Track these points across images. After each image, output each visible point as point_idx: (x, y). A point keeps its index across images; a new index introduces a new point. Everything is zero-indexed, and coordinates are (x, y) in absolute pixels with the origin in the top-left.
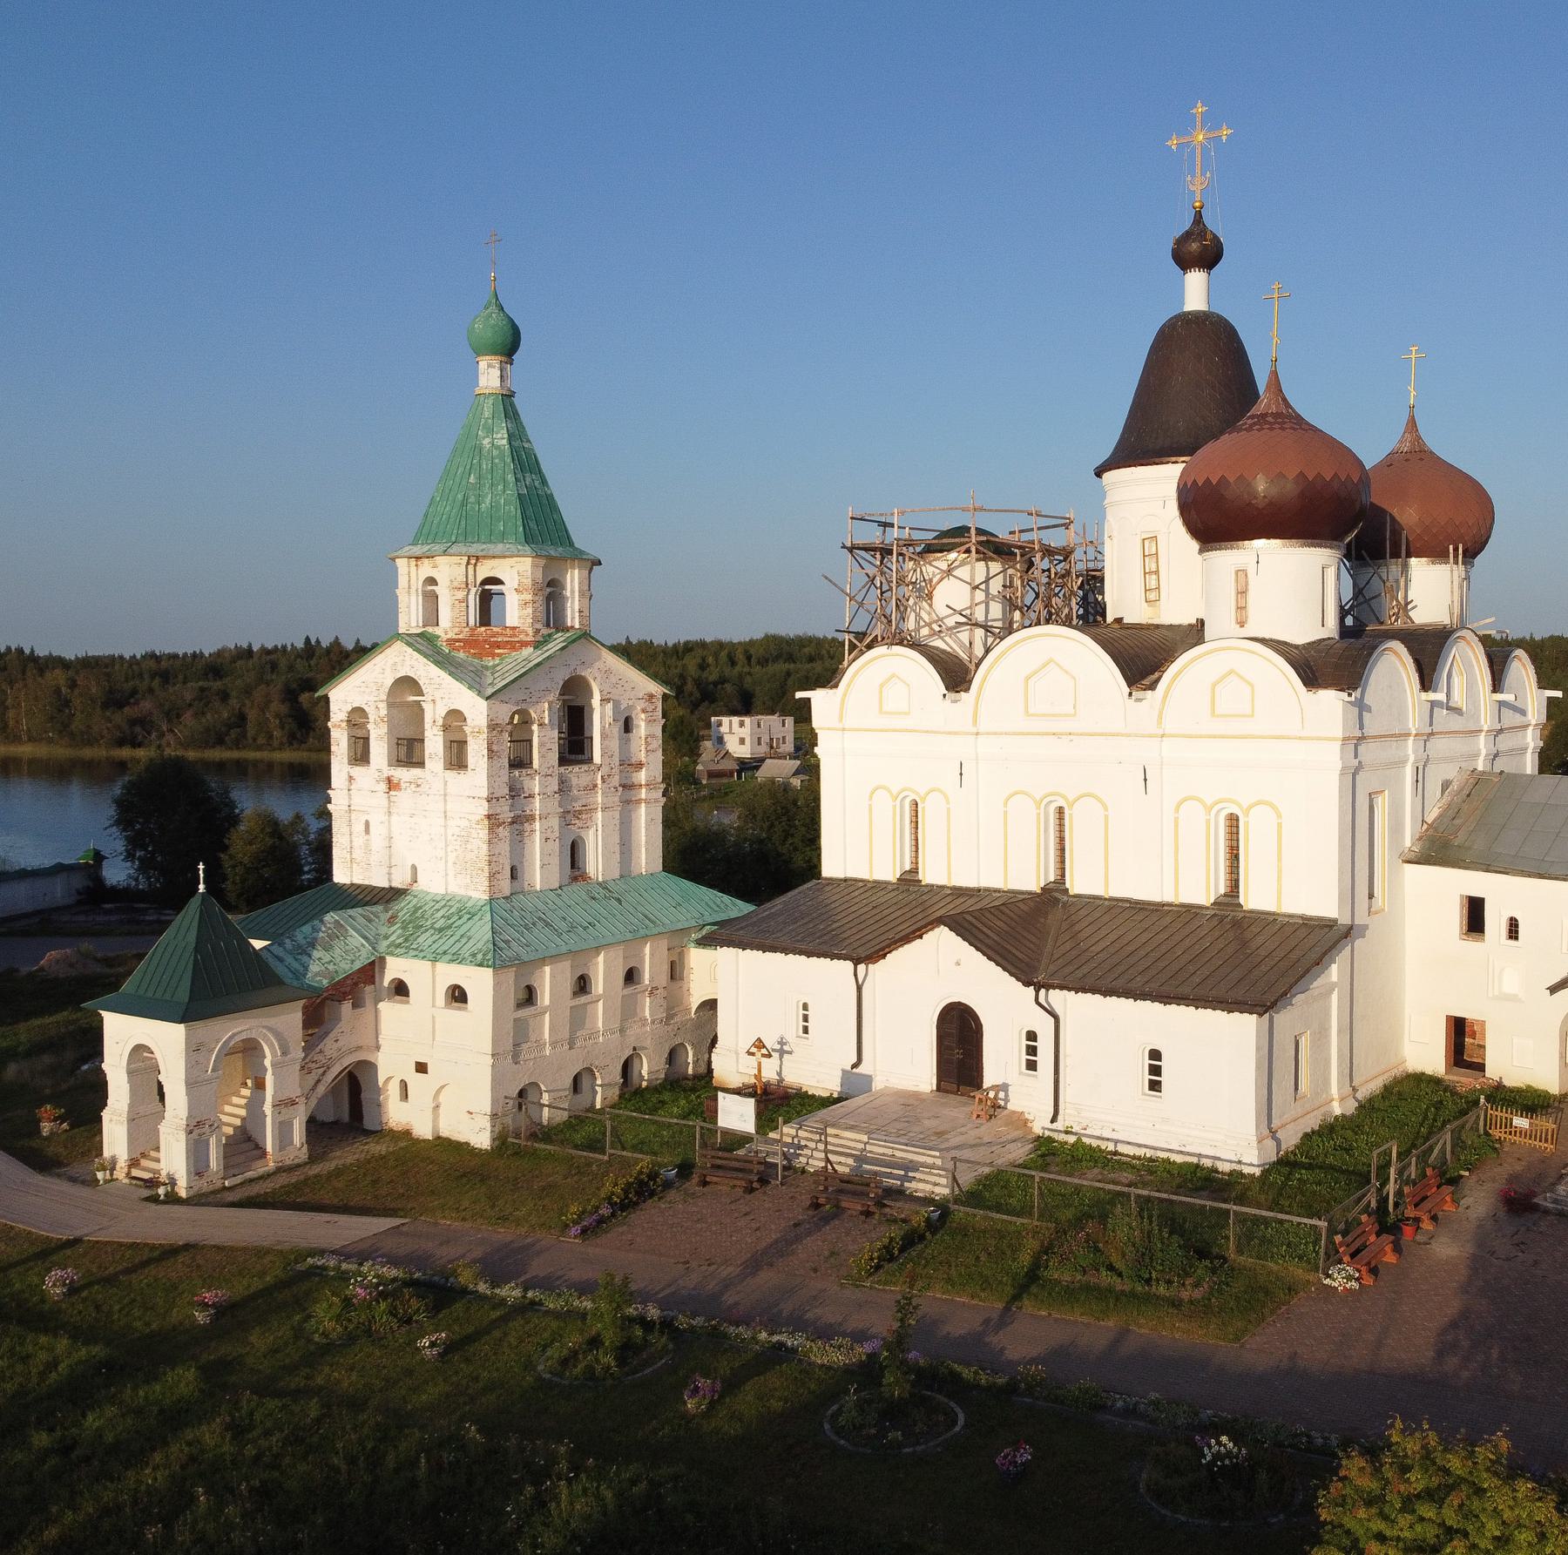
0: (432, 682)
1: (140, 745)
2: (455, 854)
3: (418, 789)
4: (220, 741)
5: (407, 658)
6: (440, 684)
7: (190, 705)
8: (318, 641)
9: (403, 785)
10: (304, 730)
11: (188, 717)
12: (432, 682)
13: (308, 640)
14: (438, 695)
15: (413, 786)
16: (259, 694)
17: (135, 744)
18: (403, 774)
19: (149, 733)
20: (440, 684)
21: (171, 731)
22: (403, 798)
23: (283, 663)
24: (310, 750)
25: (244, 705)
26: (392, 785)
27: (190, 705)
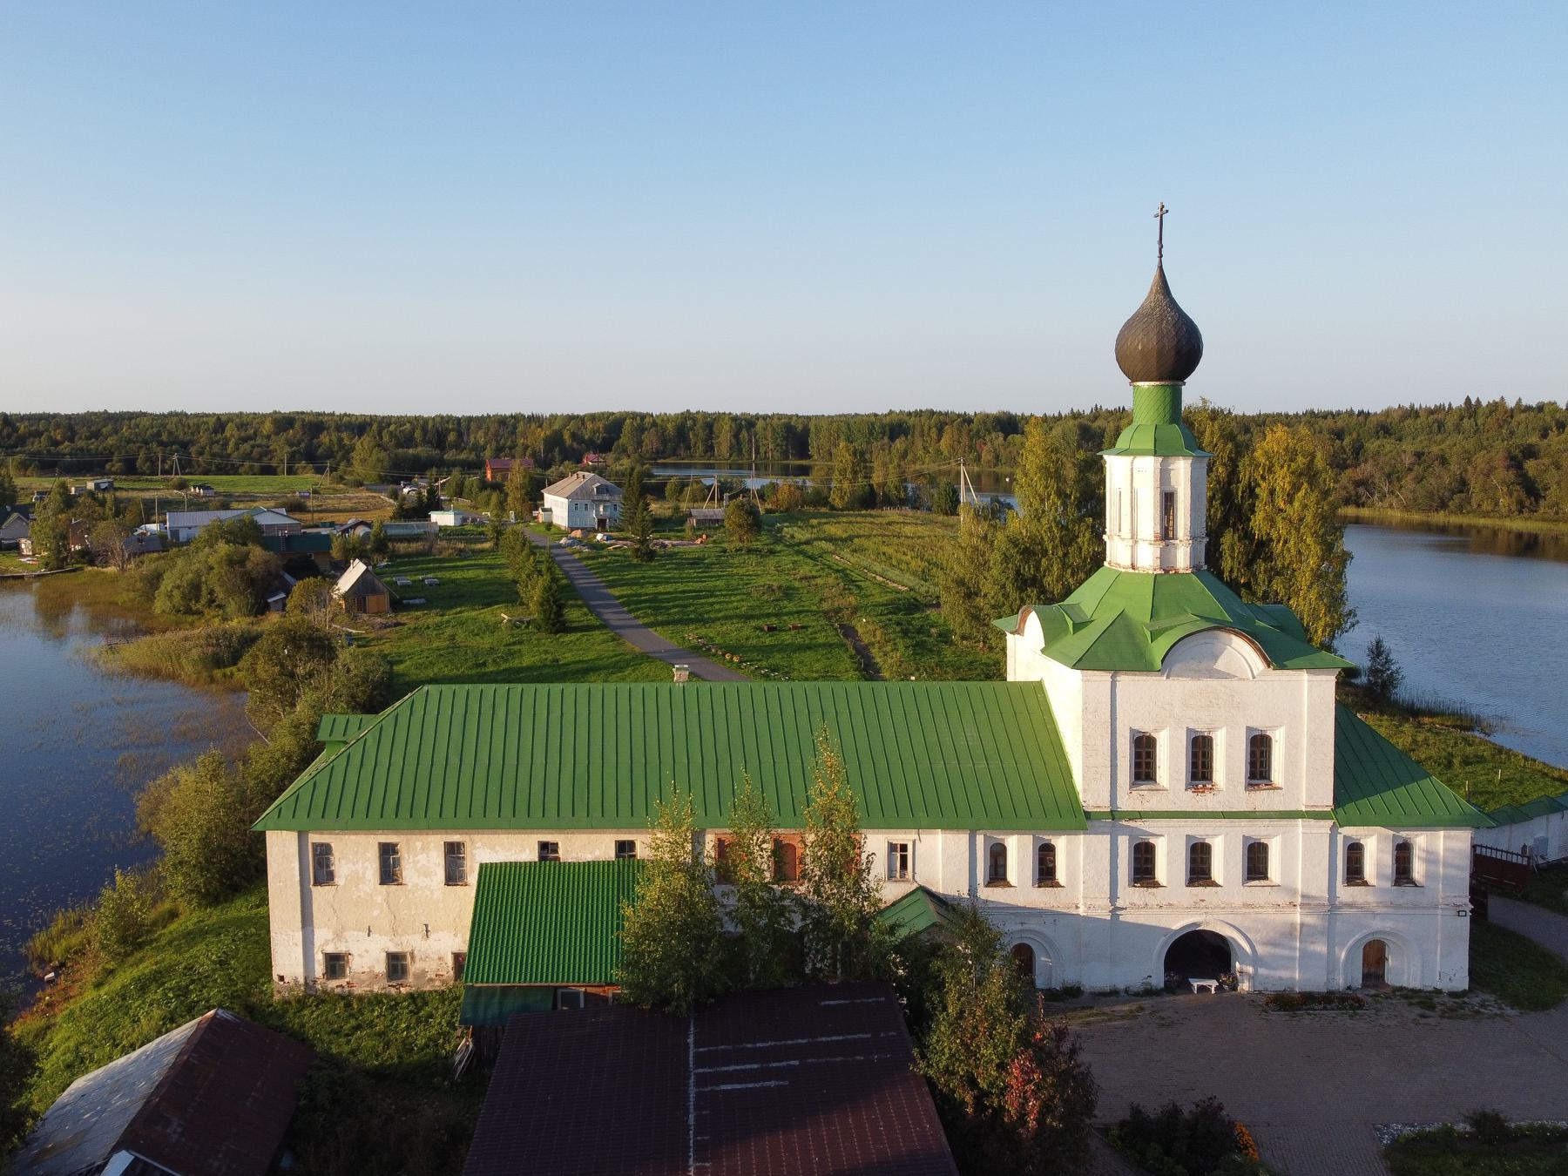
1: (1363, 505)
4: (1443, 505)
7: (1410, 470)
8: (1478, 401)
10: (1533, 499)
11: (1408, 482)
13: (1468, 400)
16: (1480, 459)
17: (1359, 504)
19: (1372, 494)
21: (1393, 493)
23: (1450, 423)
24: (1544, 520)
25: (1466, 470)
27: (1410, 470)
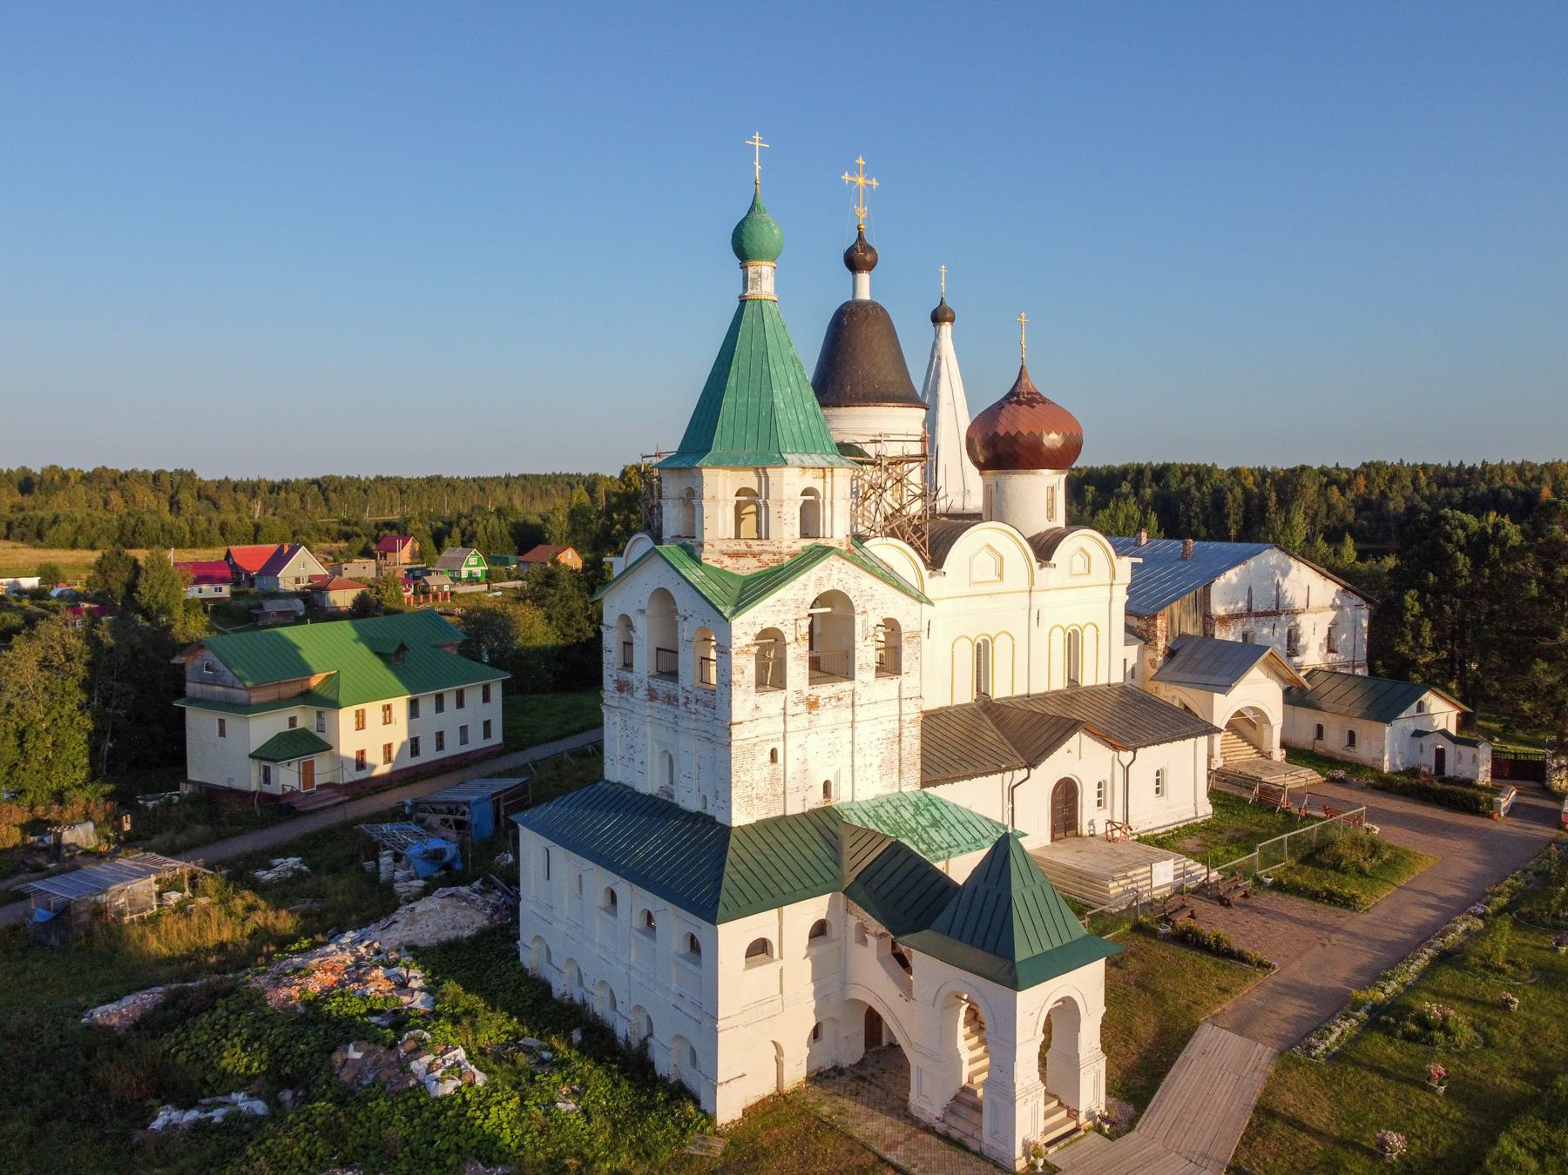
0: (864, 593)
2: (881, 757)
3: (841, 702)
5: (835, 572)
6: (873, 596)
9: (821, 702)
12: (864, 593)
14: (869, 607)
15: (833, 702)
18: (825, 691)
20: (873, 596)
22: (826, 716)
26: (813, 705)
